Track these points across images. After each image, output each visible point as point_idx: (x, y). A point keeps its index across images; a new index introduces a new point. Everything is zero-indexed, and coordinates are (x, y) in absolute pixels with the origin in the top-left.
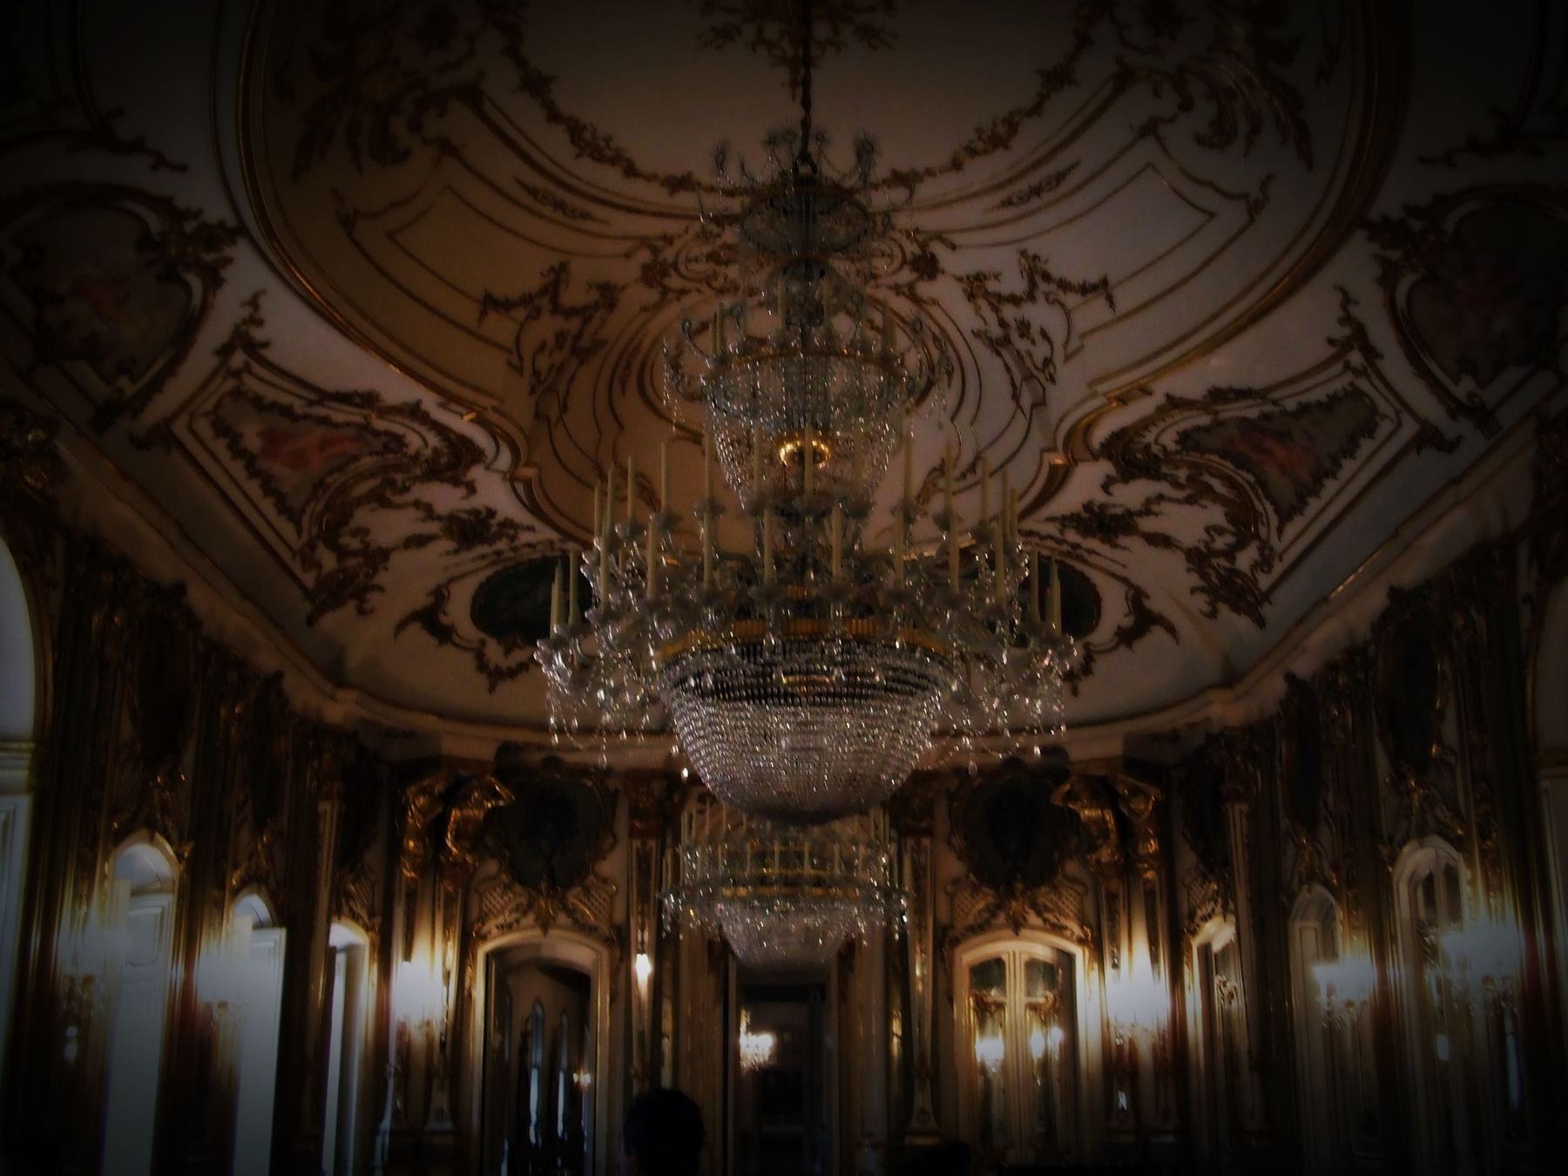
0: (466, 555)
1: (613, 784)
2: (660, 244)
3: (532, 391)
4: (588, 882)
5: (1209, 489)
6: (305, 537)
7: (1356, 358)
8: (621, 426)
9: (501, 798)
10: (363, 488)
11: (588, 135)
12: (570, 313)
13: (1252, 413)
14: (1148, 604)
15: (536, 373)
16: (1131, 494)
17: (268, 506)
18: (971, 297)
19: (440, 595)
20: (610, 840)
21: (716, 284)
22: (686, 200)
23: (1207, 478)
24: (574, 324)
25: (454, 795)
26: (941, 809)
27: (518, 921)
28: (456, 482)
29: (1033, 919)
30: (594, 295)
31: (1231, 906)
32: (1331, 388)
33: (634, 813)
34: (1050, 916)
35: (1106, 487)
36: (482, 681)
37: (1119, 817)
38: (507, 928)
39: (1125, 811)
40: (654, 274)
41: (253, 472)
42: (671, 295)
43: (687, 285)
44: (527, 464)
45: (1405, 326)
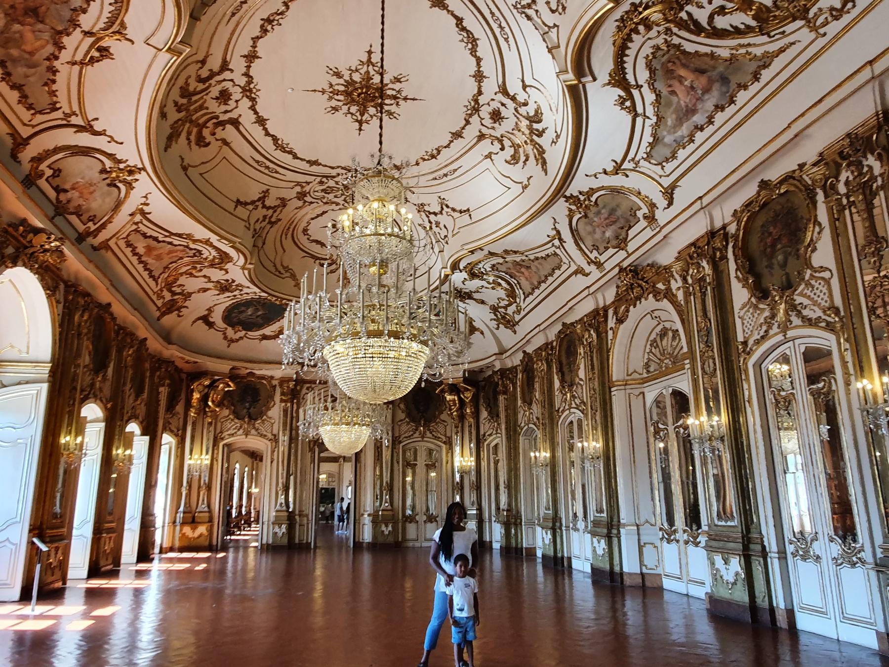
0: (222, 296)
1: (275, 382)
2: (304, 184)
3: (253, 237)
5: (500, 284)
6: (159, 287)
7: (557, 242)
8: (285, 251)
9: (231, 387)
10: (184, 269)
11: (280, 142)
12: (268, 208)
13: (518, 259)
14: (474, 323)
15: (255, 230)
16: (473, 285)
17: (145, 274)
18: (419, 211)
19: (210, 310)
20: (273, 403)
21: (325, 201)
22: (314, 169)
23: (500, 280)
24: (270, 212)
25: (212, 386)
27: (236, 433)
28: (221, 269)
30: (279, 202)
31: (499, 431)
32: (546, 252)
33: (283, 394)
35: (463, 282)
36: (226, 343)
37: (460, 399)
38: (232, 435)
39: (462, 396)
40: (301, 196)
41: (141, 262)
42: (307, 204)
43: (314, 200)
44: (250, 264)
45: (574, 232)
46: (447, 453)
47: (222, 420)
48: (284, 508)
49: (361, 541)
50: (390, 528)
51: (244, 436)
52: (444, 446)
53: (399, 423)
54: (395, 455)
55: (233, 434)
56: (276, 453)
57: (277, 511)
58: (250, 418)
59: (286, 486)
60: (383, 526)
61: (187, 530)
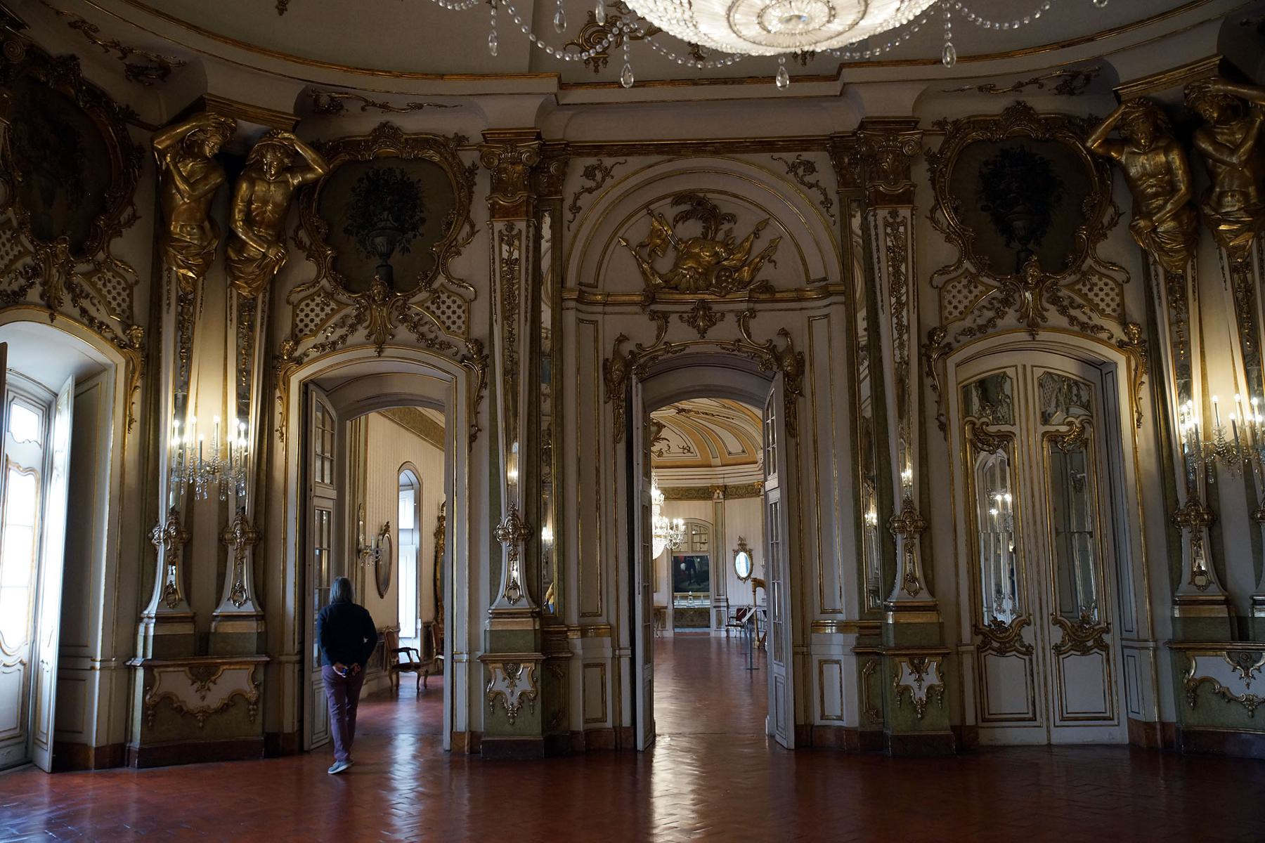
1: (468, 157)
4: (436, 285)
20: (467, 228)
26: (921, 174)
29: (1054, 317)
33: (498, 186)
34: (1073, 312)
39: (1206, 146)
46: (1134, 386)
47: (295, 298)
48: (524, 604)
49: (818, 721)
50: (932, 678)
51: (371, 351)
52: (1120, 359)
53: (939, 280)
54: (931, 397)
55: (334, 343)
56: (485, 406)
57: (497, 615)
58: (391, 283)
59: (527, 524)
60: (906, 668)
61: (178, 683)
